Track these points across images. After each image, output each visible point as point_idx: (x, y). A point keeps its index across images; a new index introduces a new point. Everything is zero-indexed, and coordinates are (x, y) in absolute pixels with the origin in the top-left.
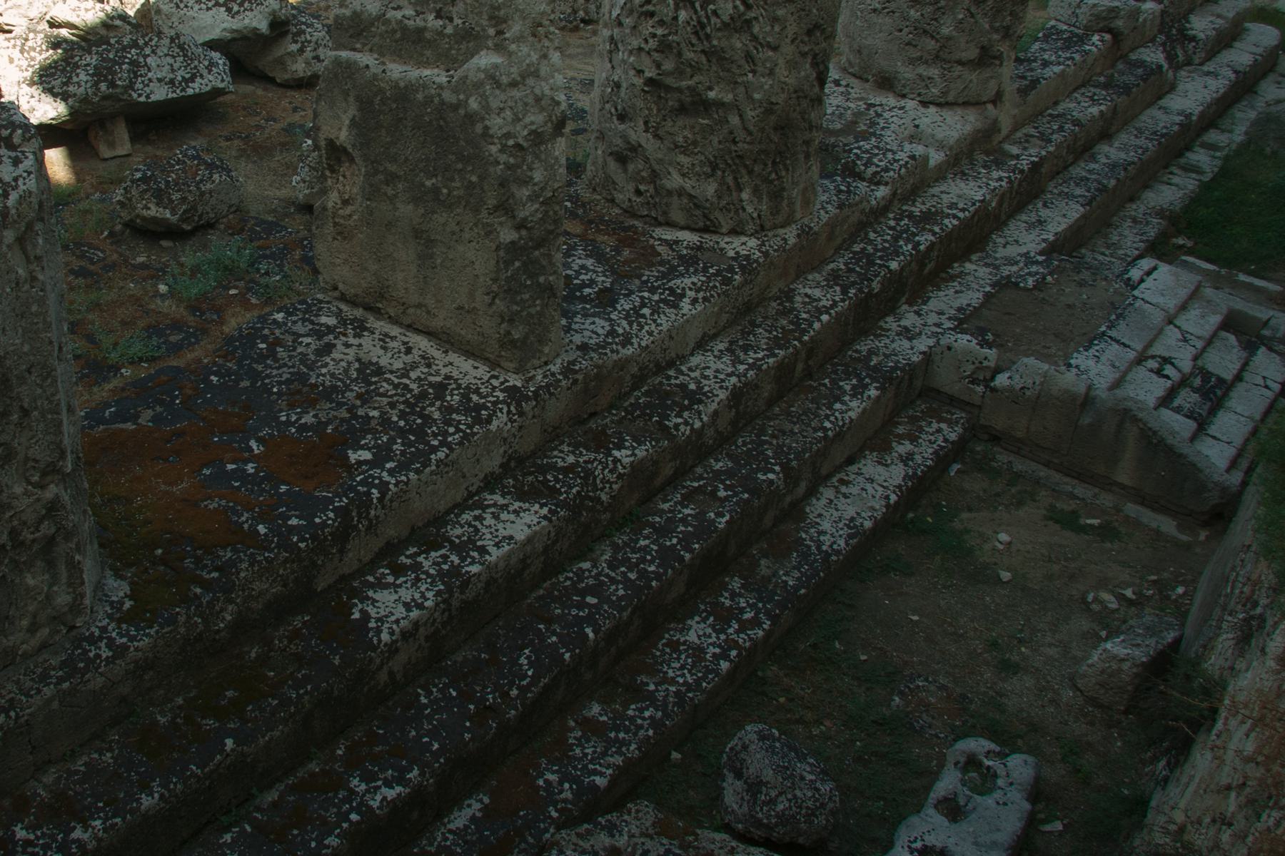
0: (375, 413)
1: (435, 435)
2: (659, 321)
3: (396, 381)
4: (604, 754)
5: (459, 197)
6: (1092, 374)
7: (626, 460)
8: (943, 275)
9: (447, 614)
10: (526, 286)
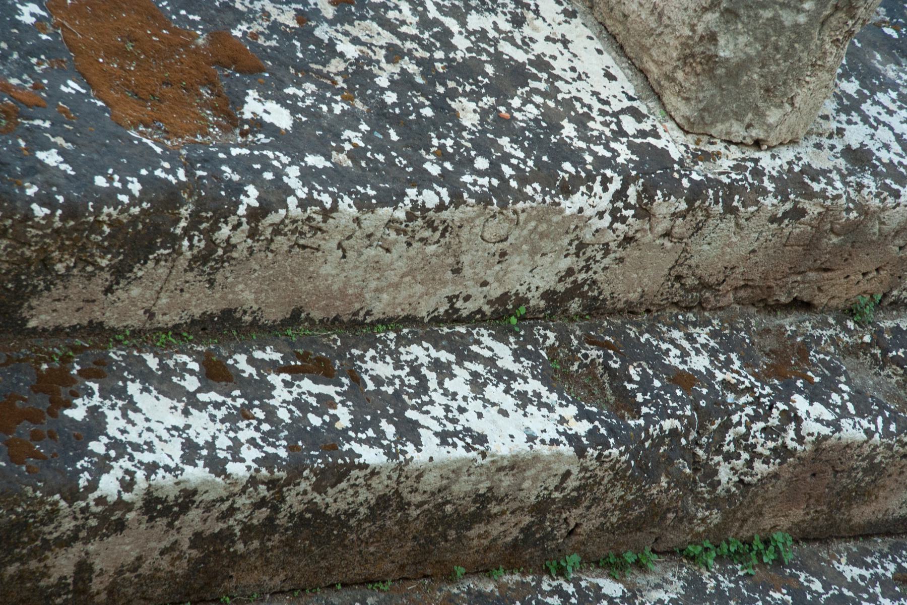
1: (442, 155)
7: (811, 427)
9: (265, 512)
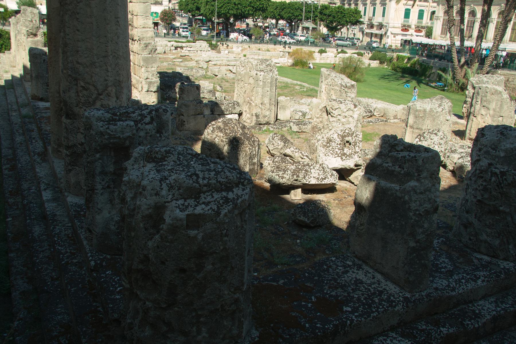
1: (374, 307)
2: (468, 285)
3: (366, 287)
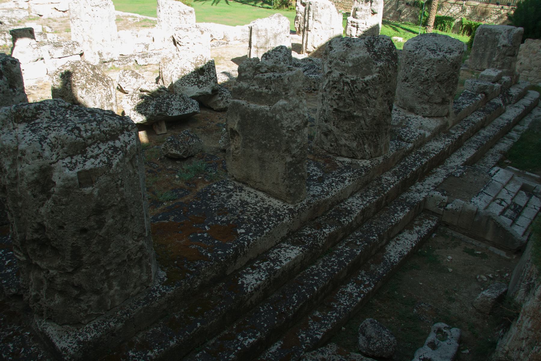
0: (246, 217)
1: (265, 224)
3: (253, 207)
4: (320, 328)
5: (273, 147)
6: (478, 205)
8: (430, 172)
9: (269, 282)
10: (295, 176)
